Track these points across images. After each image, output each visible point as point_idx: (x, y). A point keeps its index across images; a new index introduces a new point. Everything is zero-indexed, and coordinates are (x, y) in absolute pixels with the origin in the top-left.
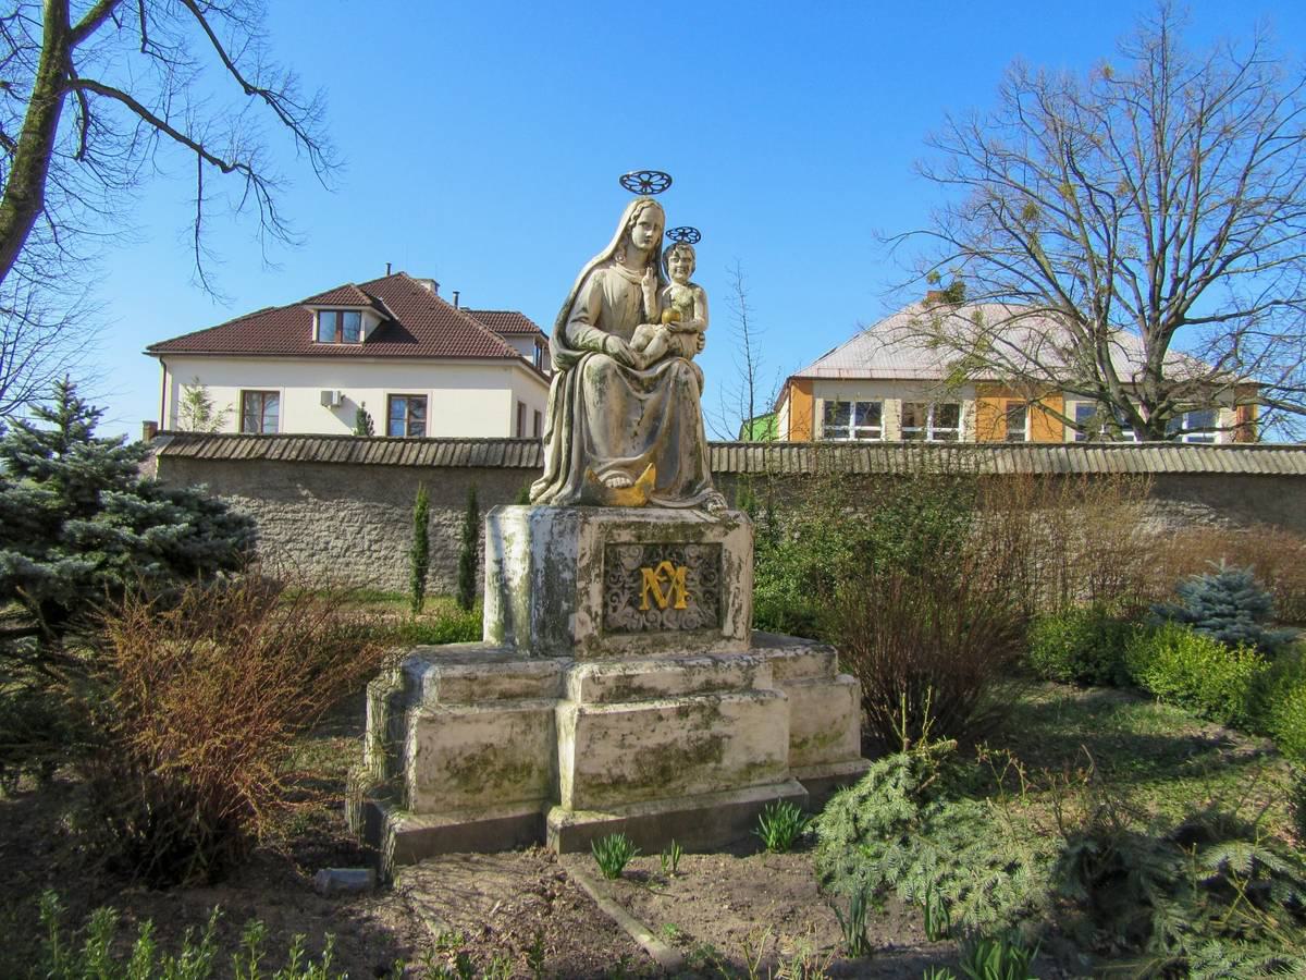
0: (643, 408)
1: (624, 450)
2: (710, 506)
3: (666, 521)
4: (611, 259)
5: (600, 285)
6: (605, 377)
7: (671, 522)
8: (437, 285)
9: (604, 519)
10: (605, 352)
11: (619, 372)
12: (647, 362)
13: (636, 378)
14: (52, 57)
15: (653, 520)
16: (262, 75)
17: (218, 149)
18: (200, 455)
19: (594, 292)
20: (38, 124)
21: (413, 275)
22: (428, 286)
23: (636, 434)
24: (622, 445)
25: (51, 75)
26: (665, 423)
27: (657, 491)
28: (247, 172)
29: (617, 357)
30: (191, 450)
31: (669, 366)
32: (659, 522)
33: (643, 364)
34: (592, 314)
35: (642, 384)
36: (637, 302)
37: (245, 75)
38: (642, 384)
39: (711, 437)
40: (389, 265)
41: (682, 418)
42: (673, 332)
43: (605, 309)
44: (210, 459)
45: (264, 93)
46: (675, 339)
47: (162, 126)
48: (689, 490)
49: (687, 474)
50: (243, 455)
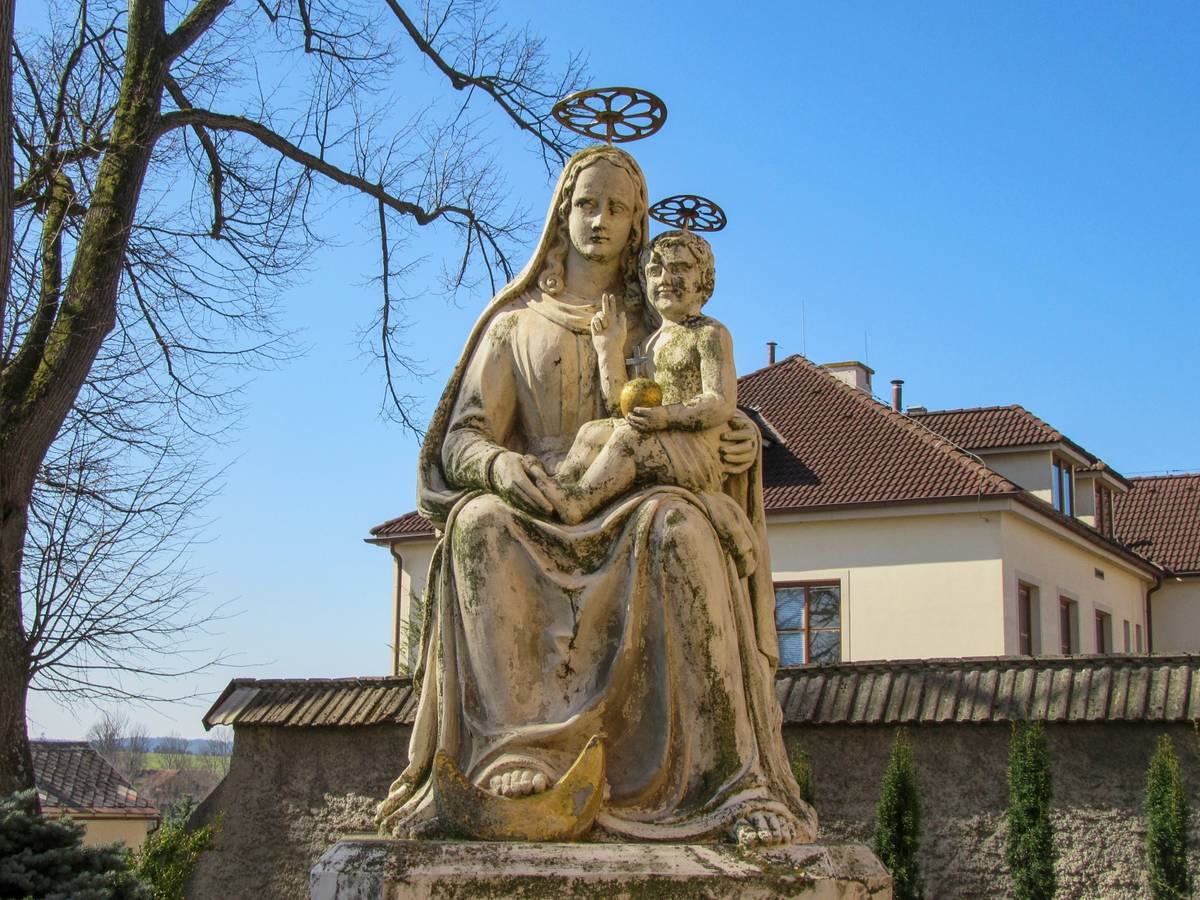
0: (575, 609)
1: (544, 708)
2: (743, 834)
3: (606, 874)
4: (531, 287)
5: (505, 345)
6: (482, 544)
7: (622, 876)
8: (869, 372)
9: (446, 870)
10: (494, 490)
11: (516, 531)
12: (586, 505)
13: (556, 542)
14: (136, 83)
15: (572, 872)
16: (481, 52)
17: (409, 186)
18: (293, 721)
19: (492, 361)
20: (111, 191)
21: (817, 357)
22: (849, 378)
23: (568, 669)
24: (538, 695)
25: (133, 111)
26: (629, 642)
27: (616, 801)
28: (466, 220)
29: (513, 497)
30: (279, 714)
31: (634, 510)
32: (590, 876)
33: (574, 509)
34: (496, 408)
35: (572, 555)
36: (586, 373)
37: (449, 59)
38: (572, 555)
39: (392, 674)
40: (773, 346)
41: (669, 625)
42: (645, 432)
43: (525, 398)
44: (308, 727)
45: (488, 84)
46: (651, 445)
47: (313, 164)
48: (703, 794)
49: (698, 757)
50: (359, 719)
